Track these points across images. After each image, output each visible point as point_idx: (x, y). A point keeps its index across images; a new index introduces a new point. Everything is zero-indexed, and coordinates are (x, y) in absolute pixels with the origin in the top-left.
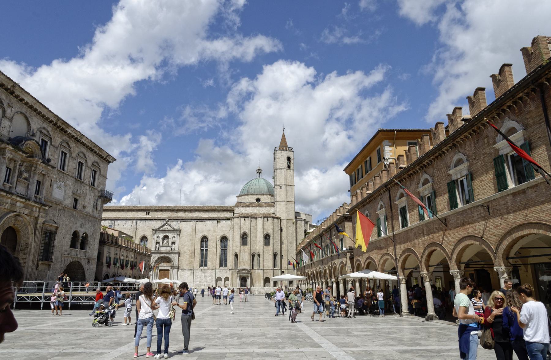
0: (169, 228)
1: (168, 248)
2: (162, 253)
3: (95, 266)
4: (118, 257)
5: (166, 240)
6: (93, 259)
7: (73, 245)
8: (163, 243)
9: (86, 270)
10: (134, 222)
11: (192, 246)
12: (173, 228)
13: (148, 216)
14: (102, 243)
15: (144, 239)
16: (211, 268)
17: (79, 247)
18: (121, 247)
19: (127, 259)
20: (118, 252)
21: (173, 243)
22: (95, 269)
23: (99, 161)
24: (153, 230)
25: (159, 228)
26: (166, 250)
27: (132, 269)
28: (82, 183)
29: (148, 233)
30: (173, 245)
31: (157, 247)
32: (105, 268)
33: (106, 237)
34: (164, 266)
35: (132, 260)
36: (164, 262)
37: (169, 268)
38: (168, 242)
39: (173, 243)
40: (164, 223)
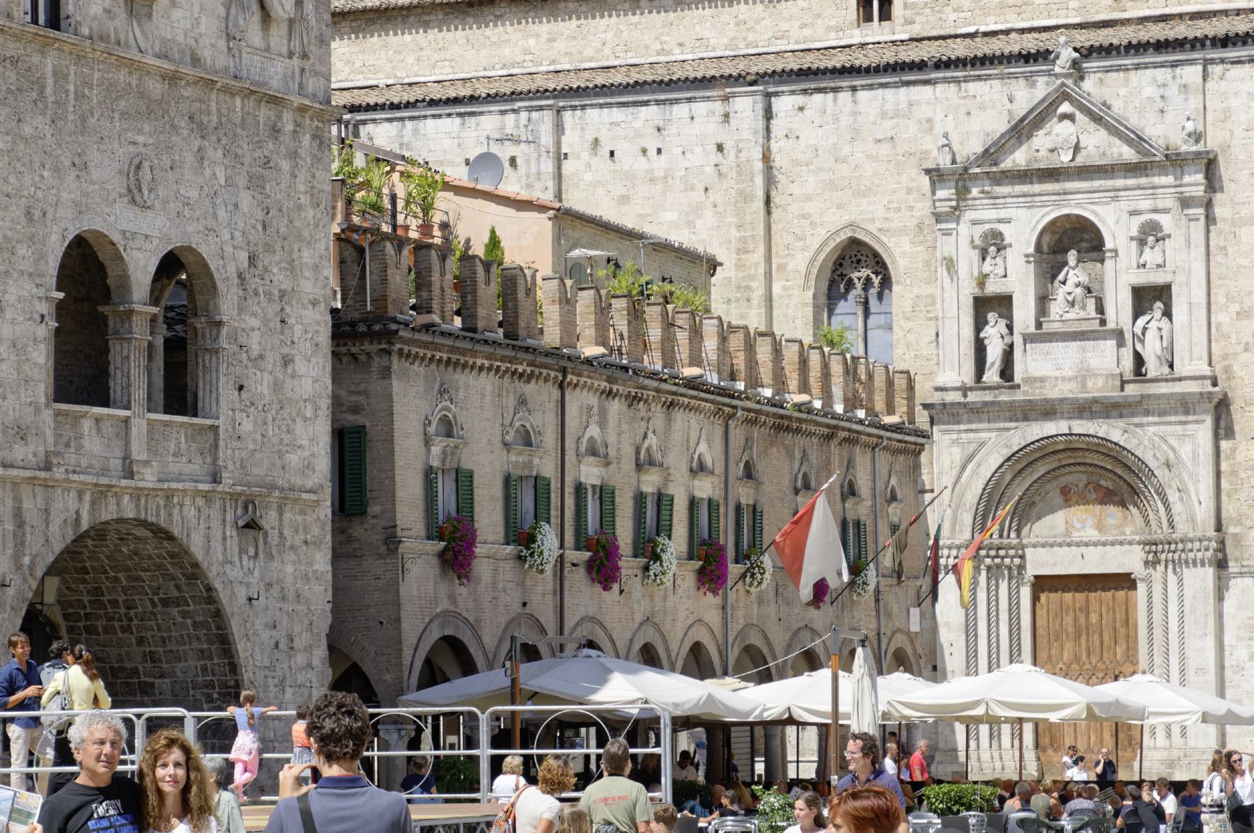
0: (1098, 145)
1: (1105, 359)
2: (1048, 410)
3: (322, 561)
4: (547, 467)
5: (1075, 274)
6: (289, 496)
7: (82, 374)
8: (1043, 301)
9: (232, 600)
10: (746, 106)
12: (1137, 140)
13: (876, 32)
14: (361, 335)
15: (854, 269)
17: (139, 393)
18: (563, 367)
19: (650, 483)
20: (543, 420)
21: (1150, 297)
22: (320, 595)
24: (936, 176)
25: (991, 154)
26: (1082, 377)
27: (711, 573)
29: (893, 215)
30: (1154, 320)
31: (994, 353)
32: (419, 575)
33: (400, 281)
34: (1074, 539)
35: (705, 488)
36: (1068, 497)
37: (1129, 560)
39: (1150, 297)
40: (1042, 88)
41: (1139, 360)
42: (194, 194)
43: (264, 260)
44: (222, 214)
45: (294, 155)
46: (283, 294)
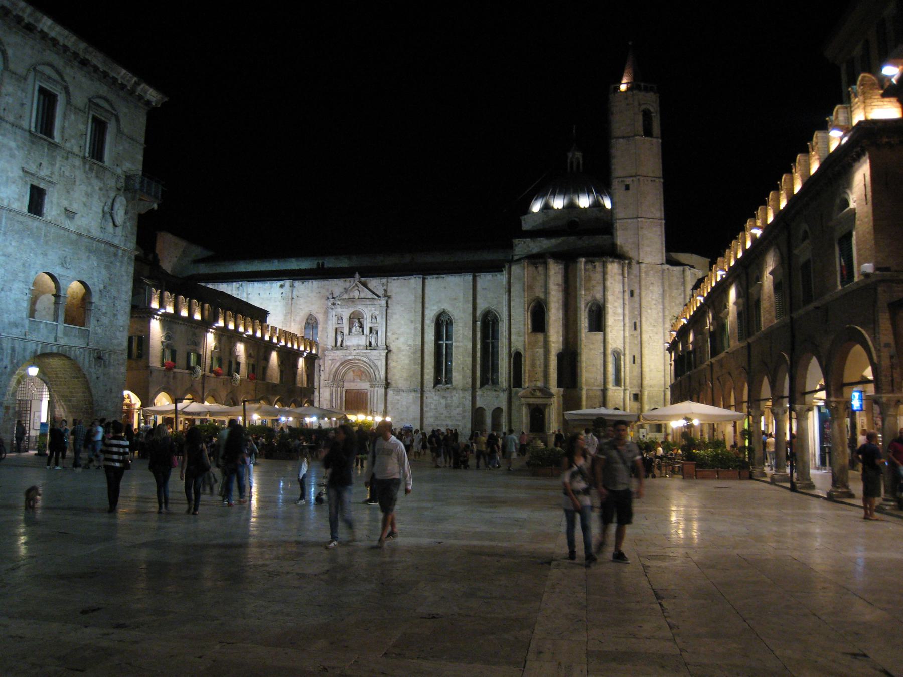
1: (363, 341)
11: (415, 335)
16: (460, 385)
23: (112, 97)
28: (54, 146)
31: (339, 340)
38: (361, 327)
41: (370, 343)
42: (85, 267)
43: (109, 288)
44: (95, 274)
45: (122, 262)
46: (115, 298)
